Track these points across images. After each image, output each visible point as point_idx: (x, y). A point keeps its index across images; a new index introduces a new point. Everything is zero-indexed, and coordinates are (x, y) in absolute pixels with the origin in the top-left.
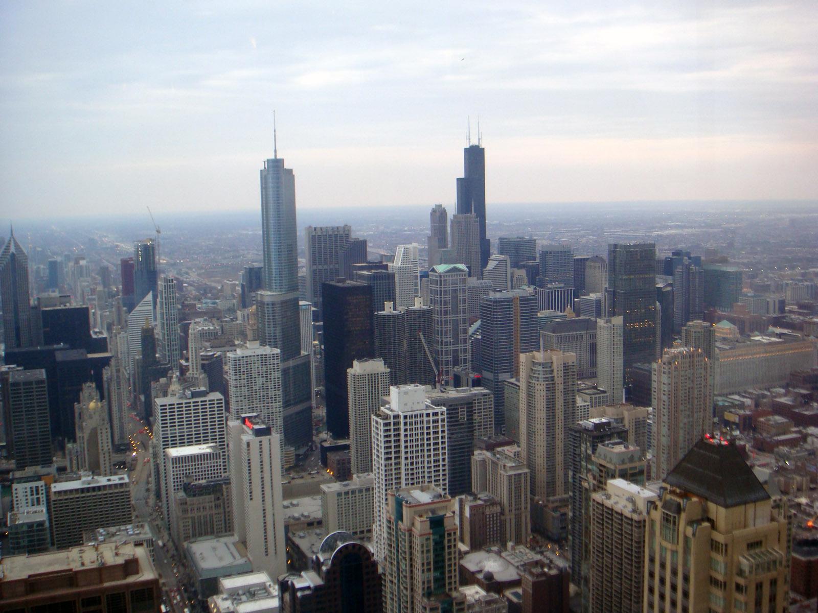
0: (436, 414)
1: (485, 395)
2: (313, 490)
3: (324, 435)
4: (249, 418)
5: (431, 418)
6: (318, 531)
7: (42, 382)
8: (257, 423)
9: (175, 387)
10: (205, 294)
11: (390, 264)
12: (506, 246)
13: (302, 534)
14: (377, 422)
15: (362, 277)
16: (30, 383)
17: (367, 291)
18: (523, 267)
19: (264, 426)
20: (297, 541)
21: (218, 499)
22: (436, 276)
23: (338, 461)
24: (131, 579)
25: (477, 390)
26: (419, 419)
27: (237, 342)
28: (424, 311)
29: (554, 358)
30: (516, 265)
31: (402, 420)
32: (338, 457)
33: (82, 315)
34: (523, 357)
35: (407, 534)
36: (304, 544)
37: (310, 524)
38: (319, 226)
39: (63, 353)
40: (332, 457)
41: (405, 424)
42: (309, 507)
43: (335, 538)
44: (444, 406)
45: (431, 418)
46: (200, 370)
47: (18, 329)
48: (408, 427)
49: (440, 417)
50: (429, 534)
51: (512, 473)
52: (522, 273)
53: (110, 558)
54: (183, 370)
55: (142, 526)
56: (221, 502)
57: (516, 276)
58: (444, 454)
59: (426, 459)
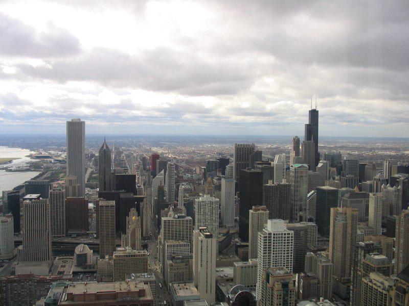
0: (289, 234)
1: (314, 226)
2: (230, 264)
3: (237, 240)
5: (286, 236)
6: (231, 284)
9: (171, 213)
10: (188, 171)
11: (272, 163)
12: (327, 157)
13: (223, 285)
14: (261, 236)
15: (259, 168)
16: (108, 206)
17: (259, 175)
18: (335, 167)
19: (209, 234)
20: (221, 287)
21: (187, 265)
23: (243, 252)
24: (141, 299)
25: (310, 224)
27: (200, 194)
28: (287, 185)
29: (348, 211)
30: (332, 166)
31: (272, 236)
32: (243, 250)
34: (332, 210)
35: (271, 289)
36: (224, 289)
37: (228, 280)
39: (123, 195)
40: (240, 250)
41: (274, 238)
42: (228, 271)
43: (237, 288)
44: (293, 230)
45: (286, 236)
46: (183, 206)
47: (105, 182)
48: (275, 239)
49: (290, 236)
51: (324, 264)
52: (335, 169)
53: (133, 289)
54: (176, 205)
55: (151, 275)
56: (188, 266)
57: (331, 170)
58: (291, 253)
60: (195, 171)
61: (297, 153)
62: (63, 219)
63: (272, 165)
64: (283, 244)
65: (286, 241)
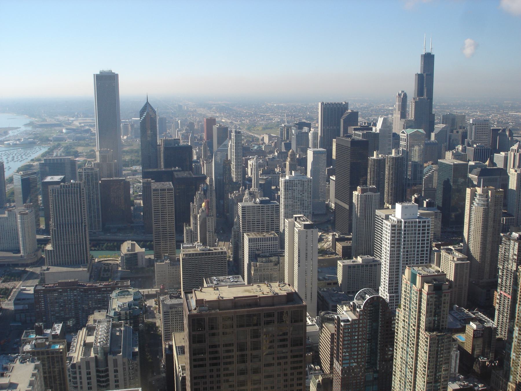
0: (425, 222)
4: (299, 217)
5: (421, 224)
7: (171, 189)
8: (304, 221)
9: (246, 196)
11: (374, 128)
12: (445, 119)
16: (164, 190)
22: (405, 136)
26: (414, 224)
33: (188, 150)
34: (468, 191)
38: (333, 102)
45: (421, 224)
49: (427, 224)
50: (433, 294)
55: (238, 277)
57: (452, 138)
59: (416, 249)
60: (263, 139)
61: (403, 115)
62: (98, 209)
63: (374, 131)
64: (417, 235)
65: (421, 232)
